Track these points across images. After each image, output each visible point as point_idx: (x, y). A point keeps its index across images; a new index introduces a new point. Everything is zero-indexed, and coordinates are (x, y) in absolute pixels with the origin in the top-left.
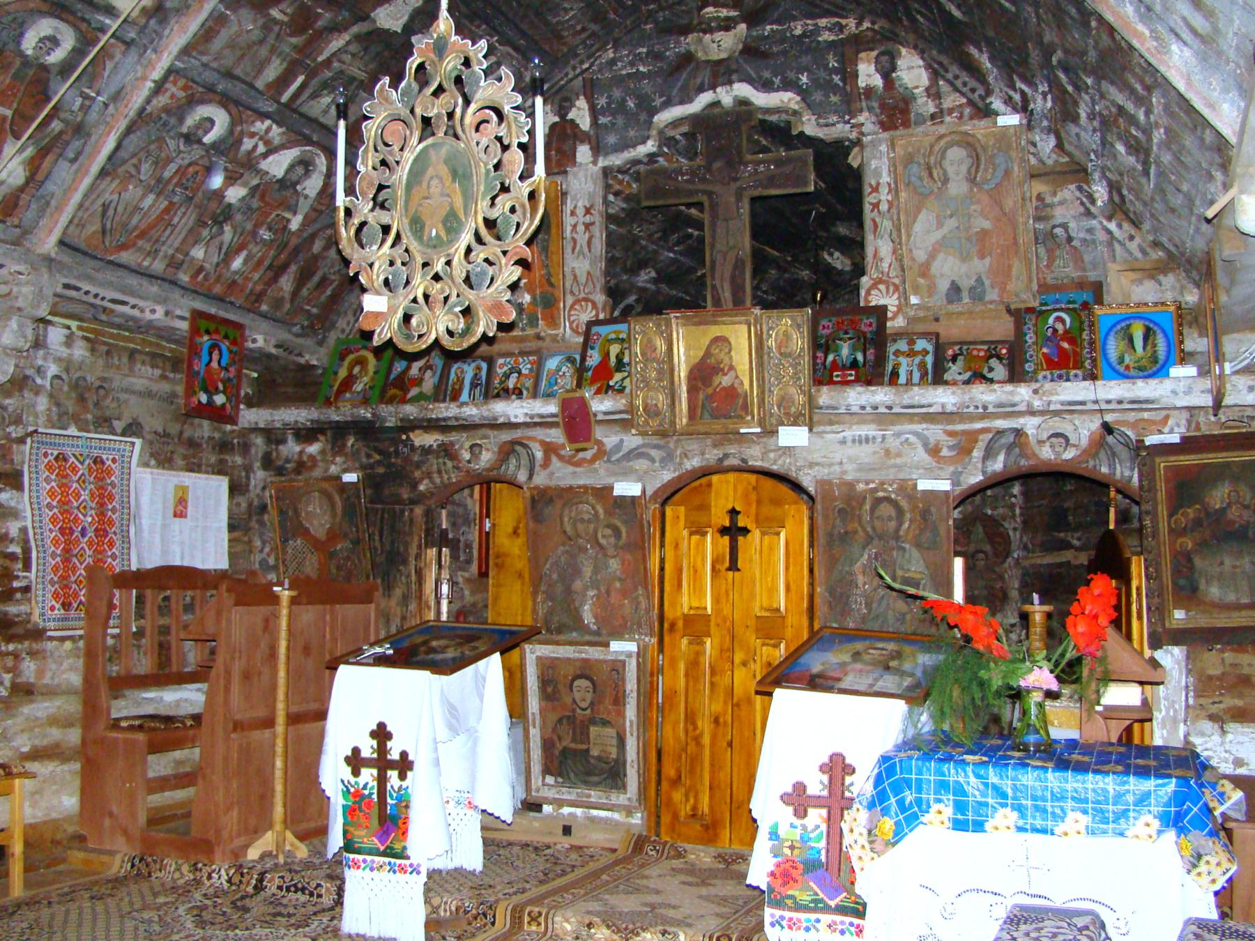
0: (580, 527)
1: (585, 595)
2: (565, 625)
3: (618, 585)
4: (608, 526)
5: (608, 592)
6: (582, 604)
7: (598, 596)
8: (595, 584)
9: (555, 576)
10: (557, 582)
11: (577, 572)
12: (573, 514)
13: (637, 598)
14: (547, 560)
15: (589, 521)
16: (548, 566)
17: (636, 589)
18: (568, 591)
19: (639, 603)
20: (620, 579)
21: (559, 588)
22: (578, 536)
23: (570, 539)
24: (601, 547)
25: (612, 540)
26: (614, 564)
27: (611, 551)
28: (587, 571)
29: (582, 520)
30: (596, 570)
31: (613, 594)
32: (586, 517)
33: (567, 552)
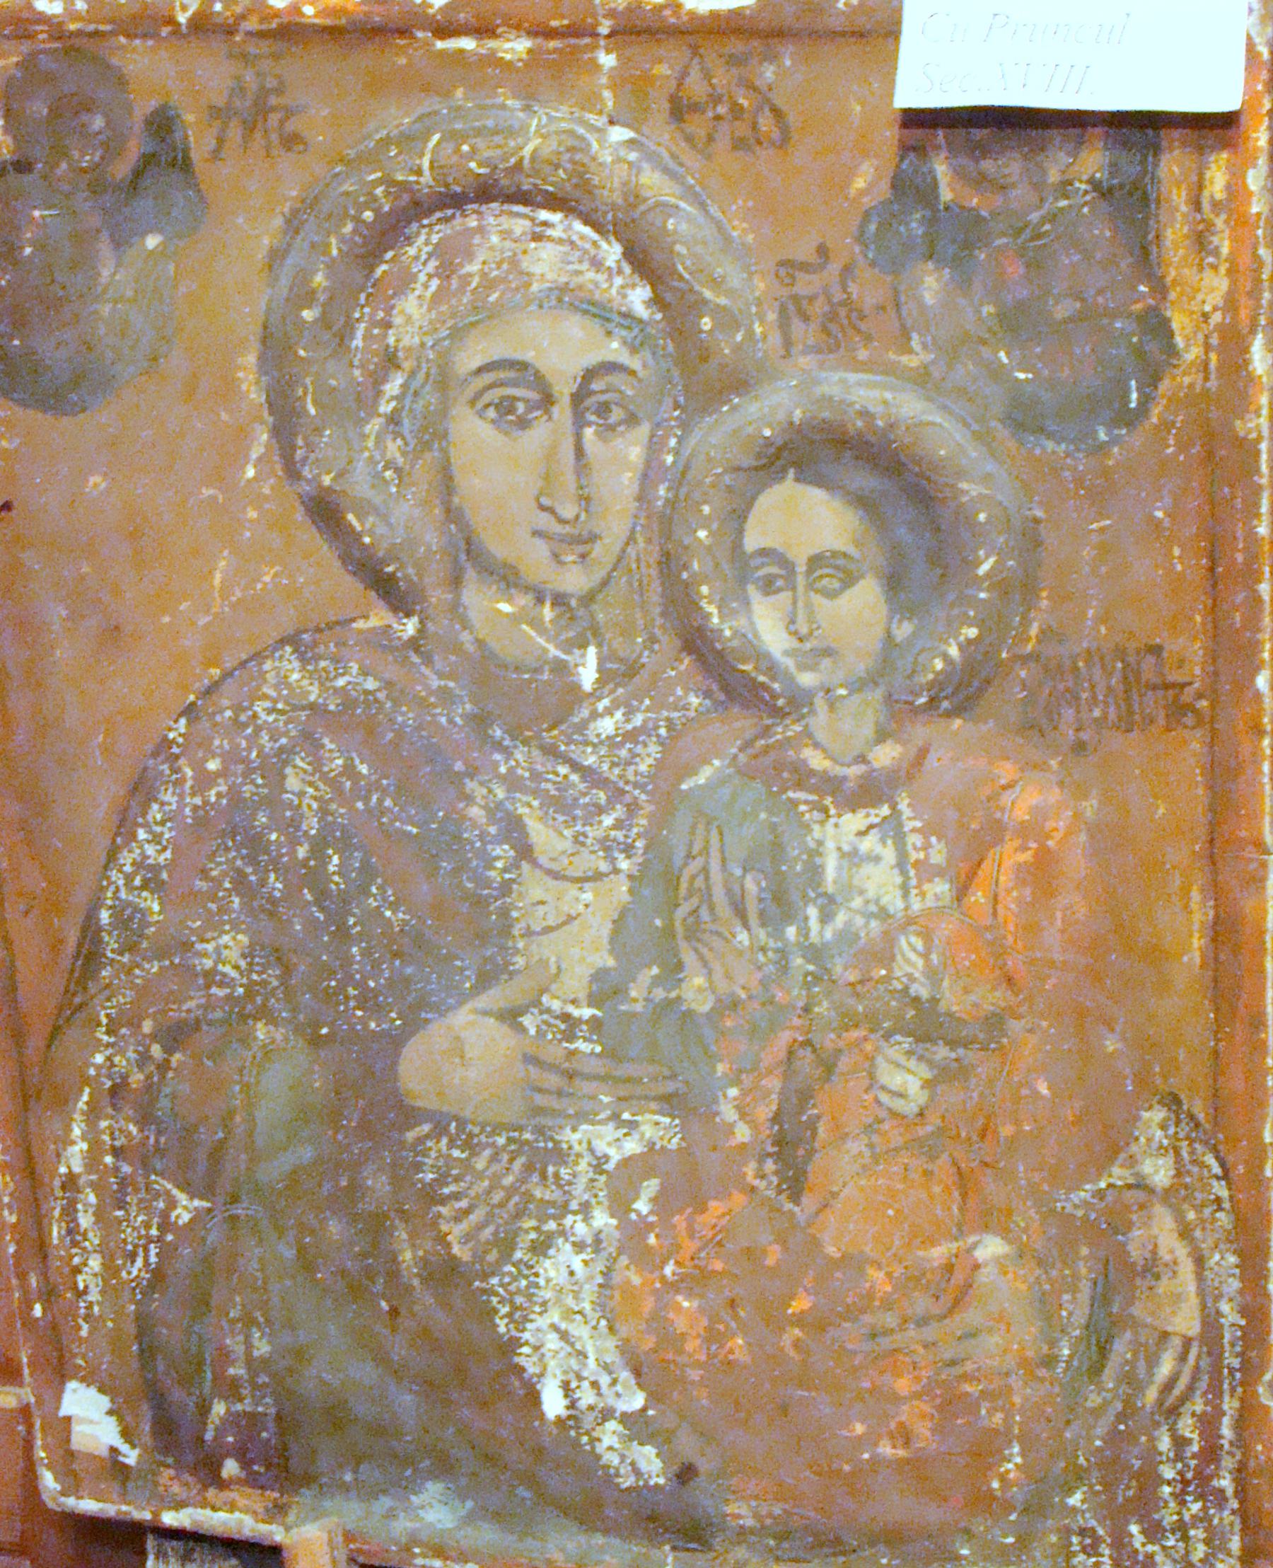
0: (498, 466)
1: (545, 1158)
2: (336, 1416)
3: (904, 1079)
4: (815, 450)
5: (791, 1148)
6: (524, 1224)
7: (685, 1182)
8: (651, 1052)
9: (226, 950)
10: (245, 1010)
11: (476, 932)
12: (413, 314)
13: (1113, 1220)
14: (142, 789)
15: (591, 397)
16: (147, 848)
17: (1113, 1144)
18: (370, 1107)
19: (1123, 1278)
20: (925, 1025)
21: (276, 1075)
22: (469, 555)
23: (389, 590)
24: (735, 682)
25: (860, 609)
26: (868, 869)
27: (842, 734)
28: (572, 921)
29: (518, 393)
30: (665, 917)
31: (844, 1164)
32: (565, 348)
33: (353, 718)
